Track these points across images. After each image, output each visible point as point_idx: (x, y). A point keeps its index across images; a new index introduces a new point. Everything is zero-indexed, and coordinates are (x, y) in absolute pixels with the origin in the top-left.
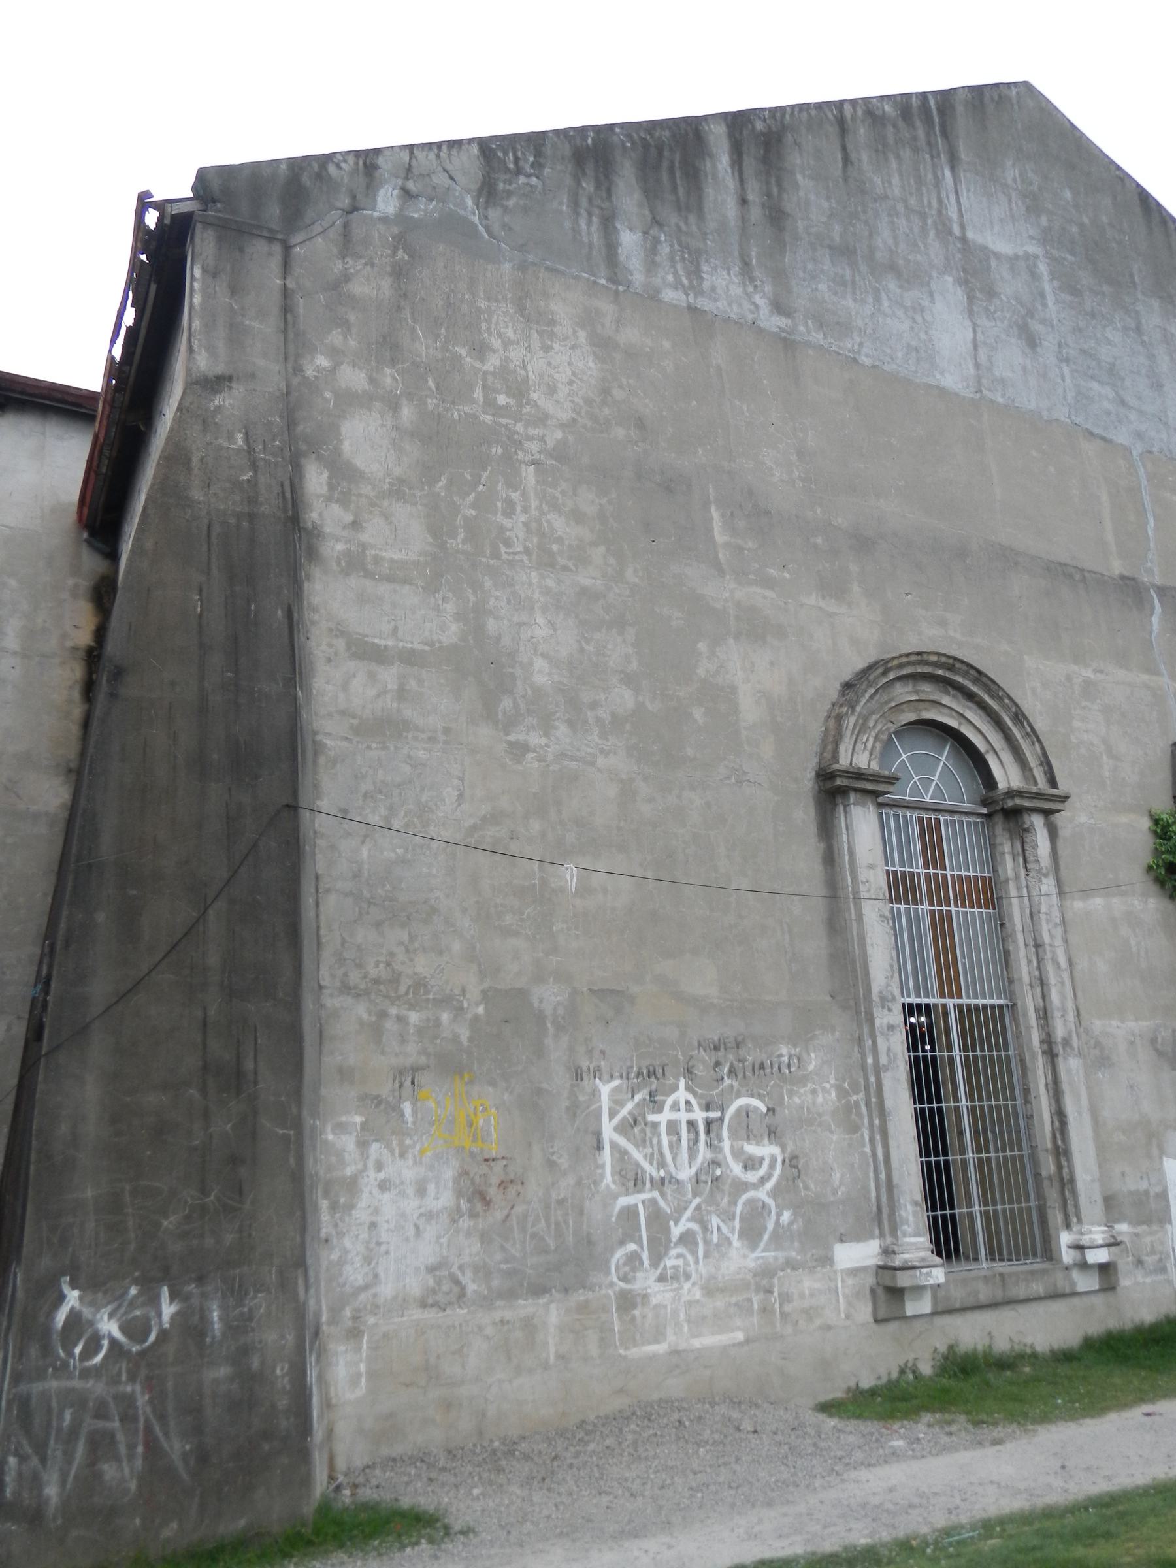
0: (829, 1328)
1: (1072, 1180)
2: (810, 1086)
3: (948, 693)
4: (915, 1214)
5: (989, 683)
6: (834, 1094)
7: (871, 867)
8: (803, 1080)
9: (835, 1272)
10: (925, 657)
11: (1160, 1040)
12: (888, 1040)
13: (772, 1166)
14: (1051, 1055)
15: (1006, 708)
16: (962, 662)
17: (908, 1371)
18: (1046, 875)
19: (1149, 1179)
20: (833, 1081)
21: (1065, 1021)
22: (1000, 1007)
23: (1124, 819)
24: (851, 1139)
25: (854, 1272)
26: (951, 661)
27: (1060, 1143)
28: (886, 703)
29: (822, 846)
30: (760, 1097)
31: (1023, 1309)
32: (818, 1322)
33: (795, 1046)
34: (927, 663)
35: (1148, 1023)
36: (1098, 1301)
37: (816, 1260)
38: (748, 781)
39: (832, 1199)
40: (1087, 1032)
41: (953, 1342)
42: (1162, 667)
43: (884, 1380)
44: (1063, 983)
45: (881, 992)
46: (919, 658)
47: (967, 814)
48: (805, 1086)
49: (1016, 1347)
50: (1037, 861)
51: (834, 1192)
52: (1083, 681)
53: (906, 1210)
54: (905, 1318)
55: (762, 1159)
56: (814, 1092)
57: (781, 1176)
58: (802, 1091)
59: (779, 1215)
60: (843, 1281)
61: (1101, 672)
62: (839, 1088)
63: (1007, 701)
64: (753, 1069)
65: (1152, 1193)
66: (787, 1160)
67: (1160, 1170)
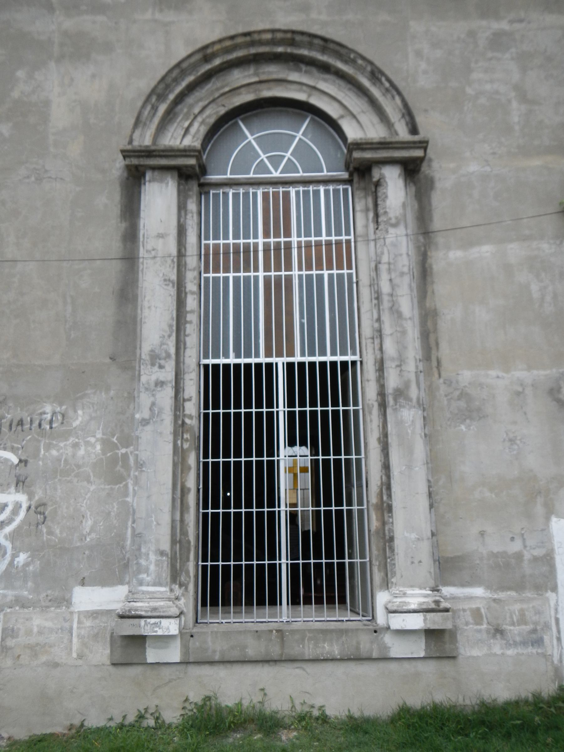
0: (56, 665)
1: (392, 539)
2: (72, 440)
3: (299, 70)
4: (158, 564)
5: (338, 48)
6: (98, 447)
7: (161, 236)
8: (65, 435)
9: (72, 613)
10: (256, 37)
12: (153, 395)
13: (15, 512)
14: (383, 406)
15: (361, 69)
16: (302, 33)
17: (148, 716)
18: (395, 225)
19: (524, 540)
20: (99, 435)
21: (401, 371)
22: (344, 364)
23: (536, 162)
24: (112, 489)
25: (95, 614)
26: (289, 35)
27: (385, 498)
28: (218, 89)
29: (124, 225)
30: (13, 450)
31: (311, 668)
32: (44, 658)
33: (61, 405)
34: (261, 43)
35: (548, 372)
36: (430, 667)
37: (50, 601)
38: (50, 177)
39: (78, 544)
40: (448, 383)
41: (211, 694)
43: (118, 720)
44: (404, 333)
45: (152, 351)
46: (248, 39)
47: (326, 182)
48: (67, 439)
49: (299, 708)
50: (386, 213)
51: (82, 538)
53: (147, 559)
54: (145, 664)
55: (6, 505)
56: (76, 446)
57: (23, 522)
58: (62, 445)
59: (14, 556)
60: (79, 622)
61: (521, 21)
62: (107, 444)
63: (360, 62)
64: (11, 425)
65: (527, 556)
66: (33, 507)
67: (546, 529)
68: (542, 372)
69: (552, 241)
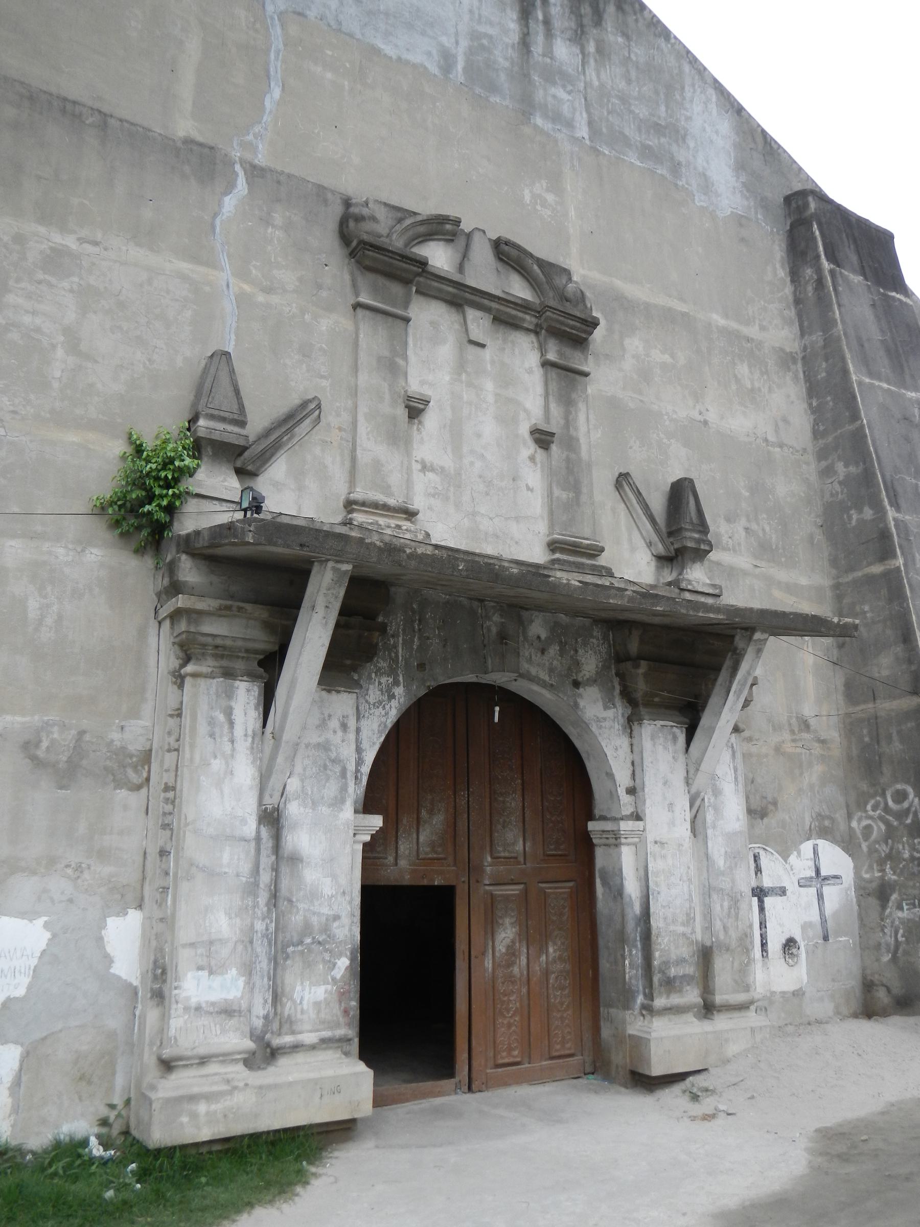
11: (45, 744)
23: (73, 437)
42: (224, 261)
52: (51, 248)
68: (19, 719)
69: (70, 546)
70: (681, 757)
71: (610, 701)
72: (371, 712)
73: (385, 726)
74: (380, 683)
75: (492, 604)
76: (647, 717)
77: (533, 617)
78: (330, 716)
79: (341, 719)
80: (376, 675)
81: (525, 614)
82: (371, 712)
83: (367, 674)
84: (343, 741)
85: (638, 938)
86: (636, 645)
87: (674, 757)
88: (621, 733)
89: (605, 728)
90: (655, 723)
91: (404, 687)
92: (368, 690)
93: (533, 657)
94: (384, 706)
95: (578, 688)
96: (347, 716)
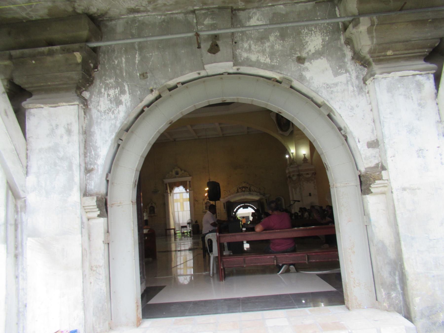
70: (431, 104)
71: (340, 67)
72: (102, 118)
73: (115, 126)
74: (109, 95)
75: (203, 12)
76: (378, 72)
77: (251, 15)
78: (57, 126)
79: (66, 126)
80: (105, 90)
81: (242, 14)
82: (102, 118)
83: (97, 90)
84: (68, 143)
85: (397, 282)
86: (355, 6)
87: (420, 105)
88: (356, 93)
89: (337, 92)
90: (392, 74)
91: (130, 94)
92: (99, 102)
93: (253, 47)
94: (113, 112)
95: (303, 63)
96: (71, 124)
